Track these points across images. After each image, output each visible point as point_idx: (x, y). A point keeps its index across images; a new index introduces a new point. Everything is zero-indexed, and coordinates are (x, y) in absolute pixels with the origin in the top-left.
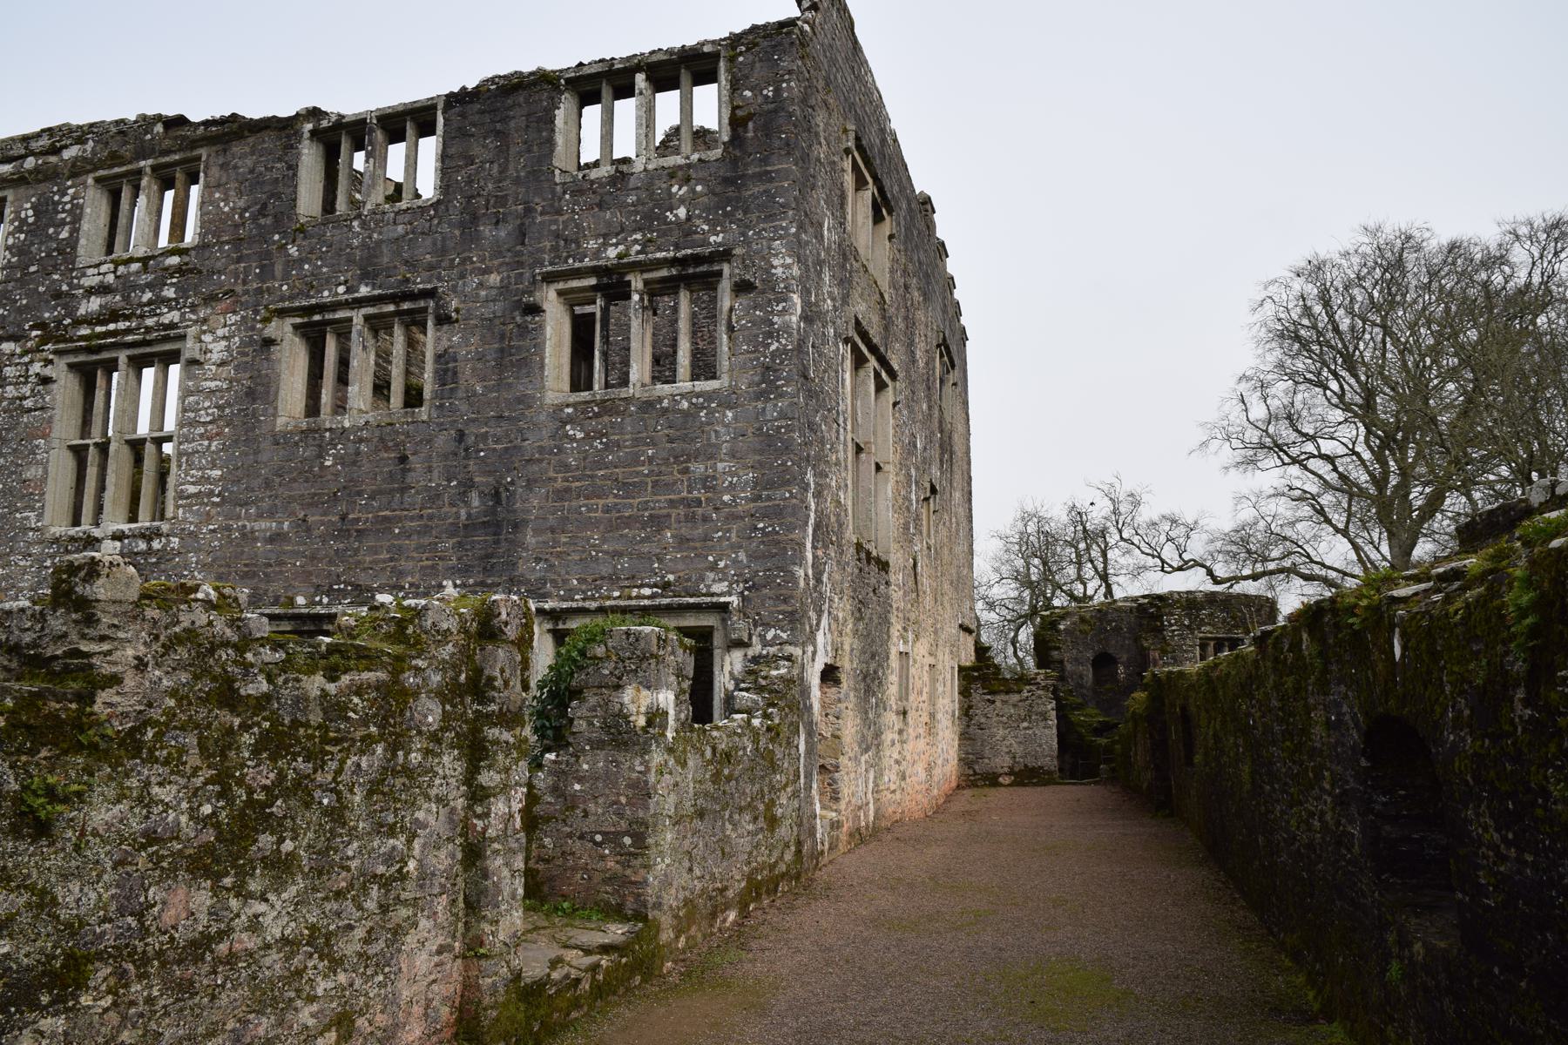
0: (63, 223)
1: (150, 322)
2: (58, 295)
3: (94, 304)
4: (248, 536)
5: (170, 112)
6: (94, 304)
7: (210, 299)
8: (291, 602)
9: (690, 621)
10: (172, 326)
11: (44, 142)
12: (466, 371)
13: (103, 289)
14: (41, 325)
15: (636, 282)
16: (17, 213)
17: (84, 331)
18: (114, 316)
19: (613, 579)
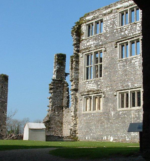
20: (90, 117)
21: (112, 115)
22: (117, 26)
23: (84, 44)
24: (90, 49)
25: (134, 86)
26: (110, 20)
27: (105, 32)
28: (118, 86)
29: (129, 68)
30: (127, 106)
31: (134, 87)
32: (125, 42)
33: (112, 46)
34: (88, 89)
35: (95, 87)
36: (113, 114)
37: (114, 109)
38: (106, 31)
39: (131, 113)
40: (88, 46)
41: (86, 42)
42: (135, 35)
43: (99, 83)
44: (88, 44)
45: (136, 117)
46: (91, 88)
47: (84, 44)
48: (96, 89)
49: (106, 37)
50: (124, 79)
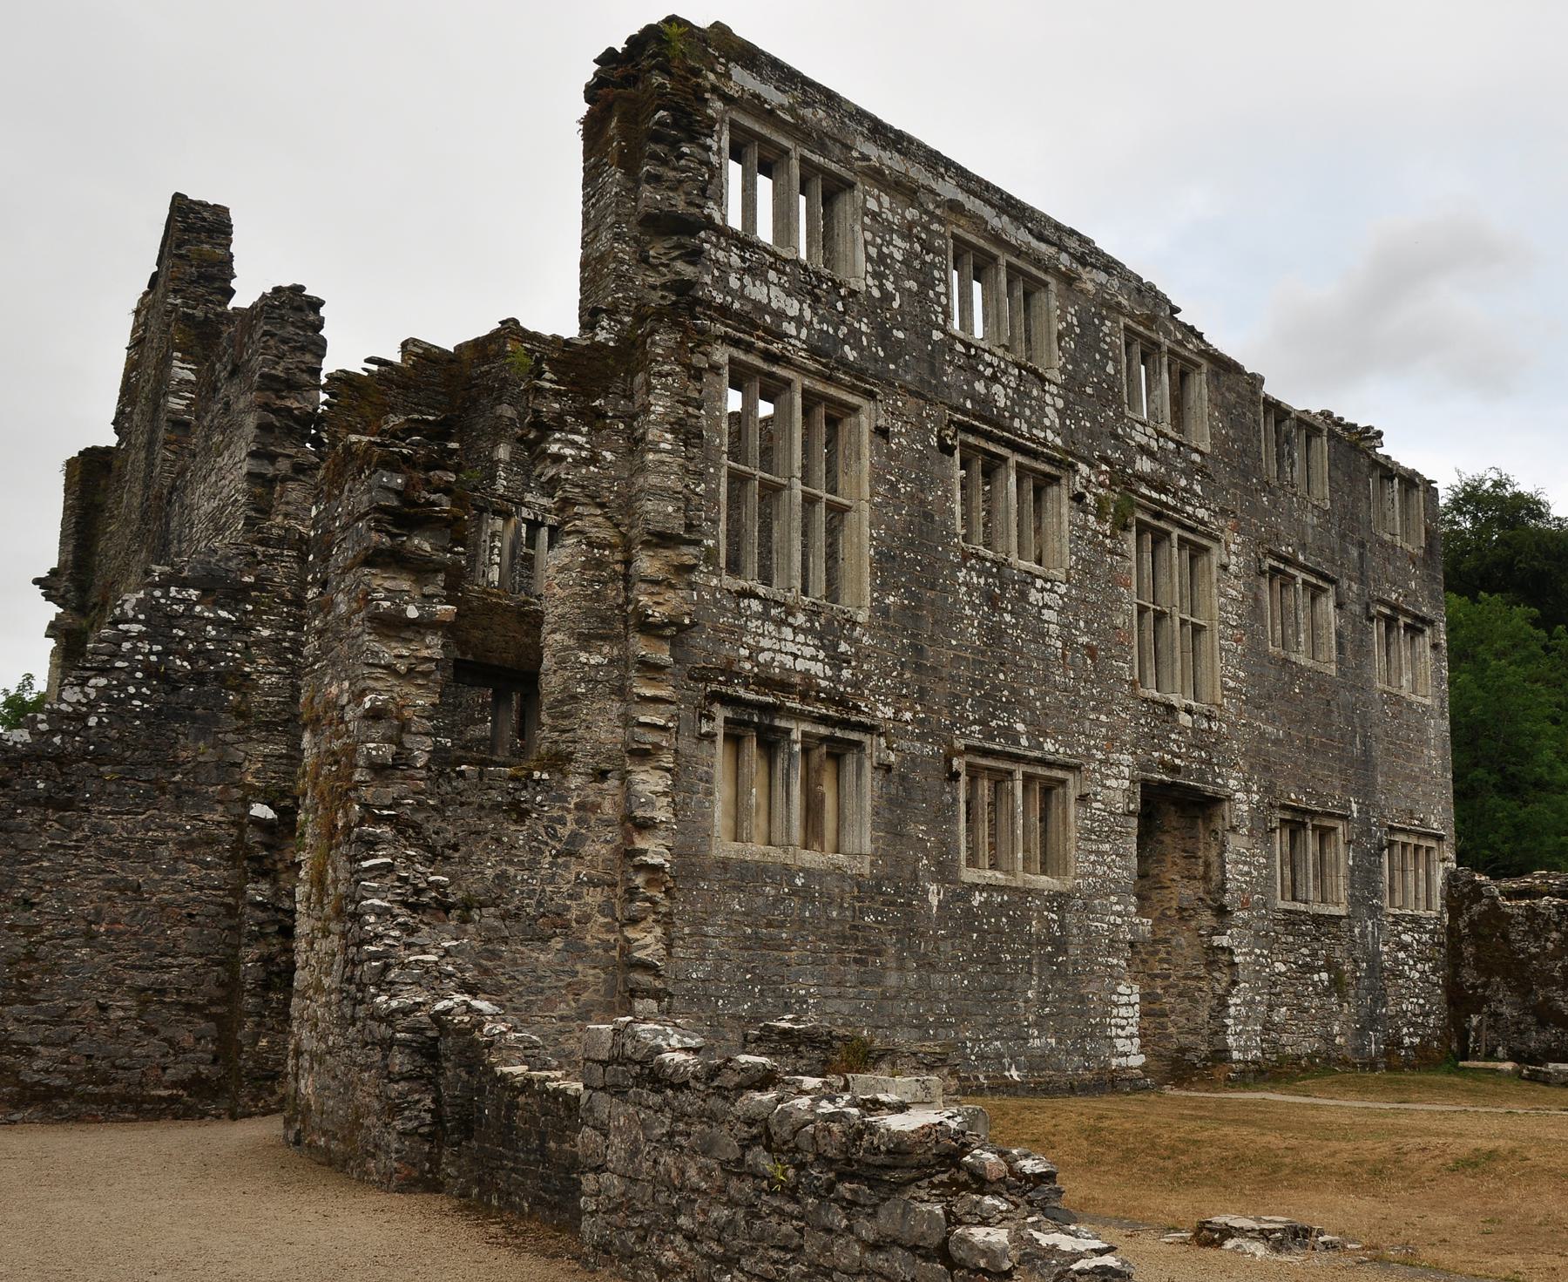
1: (1189, 509)
10: (1202, 522)
20: (778, 900)
21: (931, 908)
25: (1040, 747)
27: (876, 293)
28: (961, 716)
29: (1014, 626)
31: (1037, 754)
32: (992, 447)
34: (762, 658)
35: (817, 668)
37: (945, 872)
39: (1030, 909)
41: (735, 260)
43: (843, 647)
44: (758, 292)
45: (1053, 940)
46: (789, 661)
48: (824, 683)
50: (994, 687)
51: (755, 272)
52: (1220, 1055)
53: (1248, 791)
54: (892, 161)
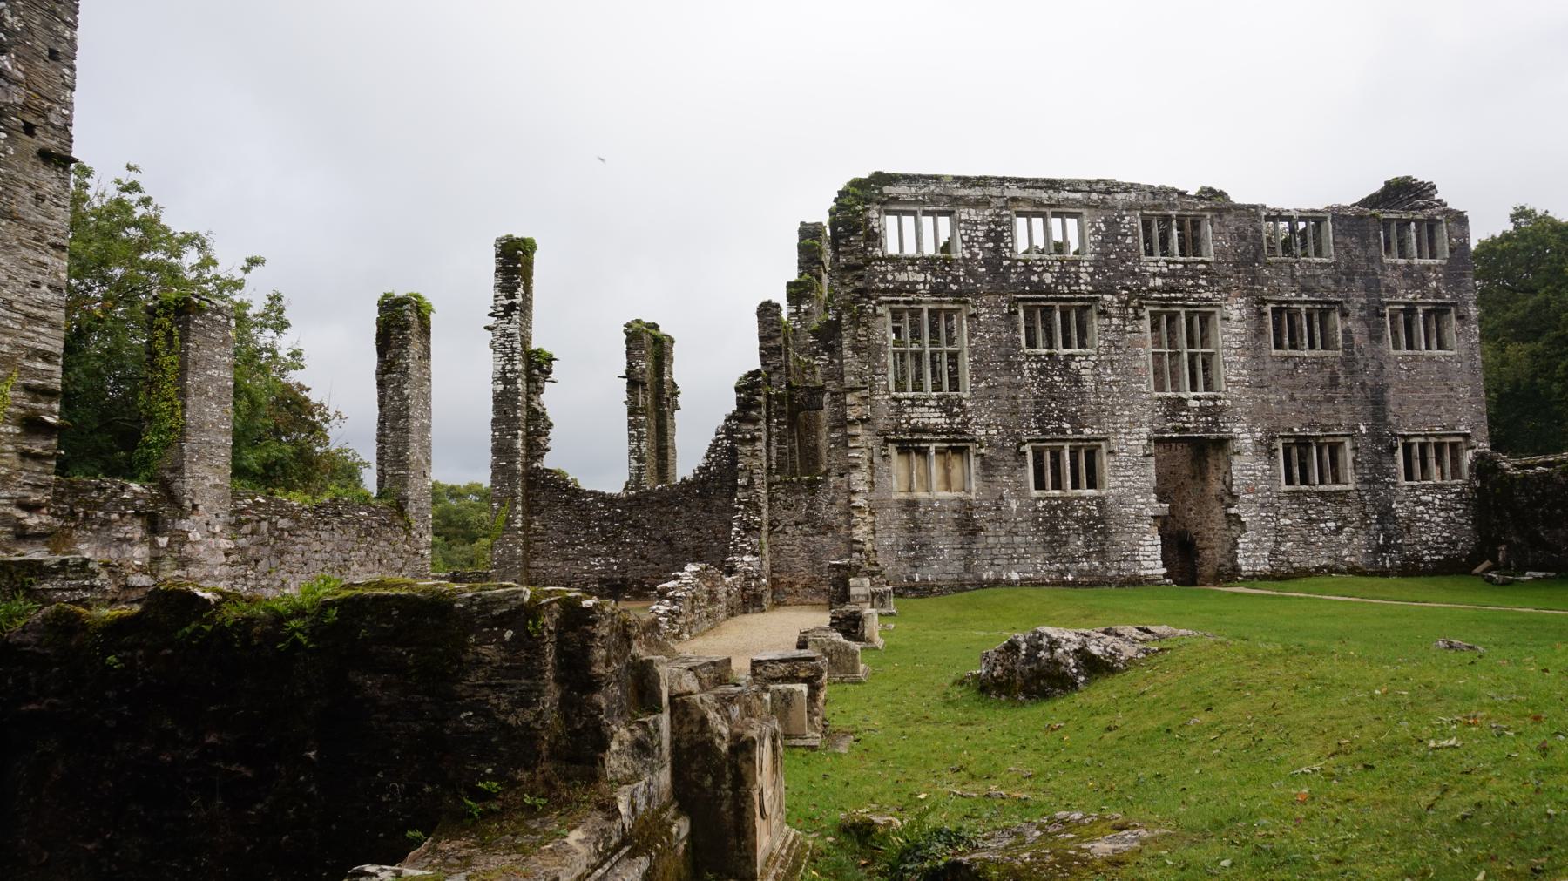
0: (1125, 235)
2: (1134, 274)
3: (1159, 282)
4: (1266, 401)
5: (1181, 189)
6: (1159, 282)
7: (1227, 290)
8: (1291, 430)
9: (1453, 439)
10: (1207, 299)
11: (1101, 186)
12: (1357, 338)
13: (1162, 275)
14: (1127, 288)
15: (1420, 309)
16: (1093, 224)
17: (1156, 295)
18: (1172, 290)
19: (1425, 423)
22: (1012, 250)
23: (885, 273)
24: (914, 297)
26: (982, 224)
30: (1057, 485)
33: (997, 305)
36: (1014, 507)
37: (1020, 492)
38: (974, 255)
40: (905, 283)
41: (890, 267)
42: (1075, 292)
44: (903, 277)
45: (1094, 518)
47: (885, 273)
49: (969, 273)
51: (902, 269)
52: (1236, 569)
53: (1251, 431)
54: (975, 193)
